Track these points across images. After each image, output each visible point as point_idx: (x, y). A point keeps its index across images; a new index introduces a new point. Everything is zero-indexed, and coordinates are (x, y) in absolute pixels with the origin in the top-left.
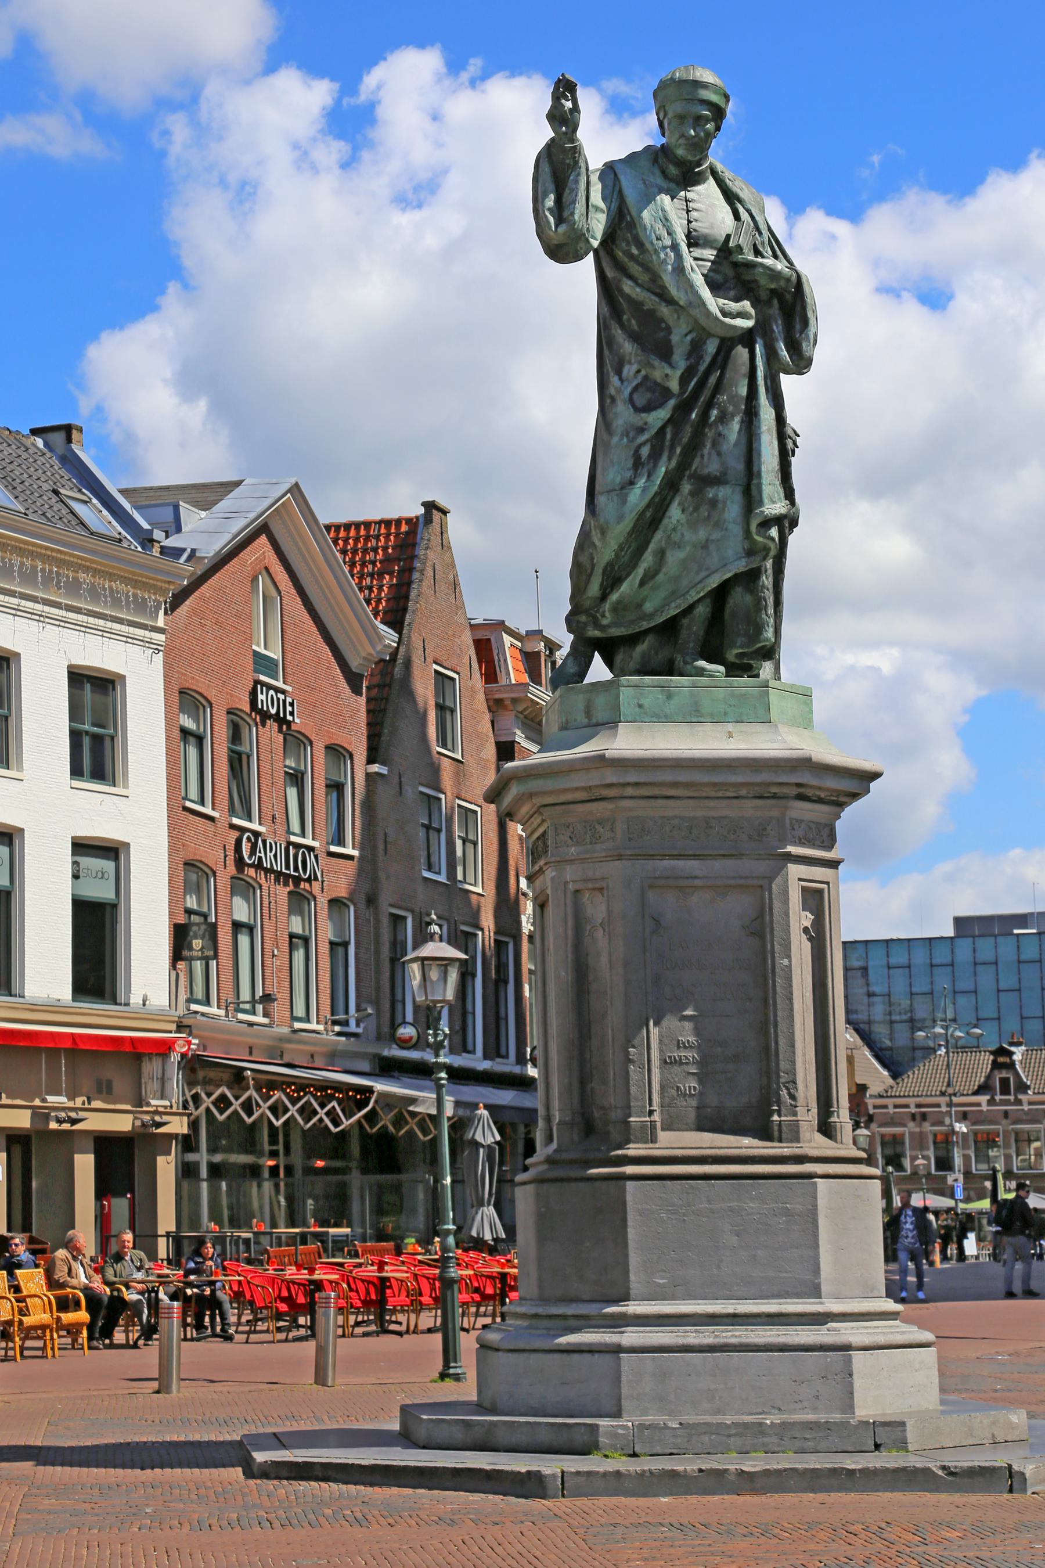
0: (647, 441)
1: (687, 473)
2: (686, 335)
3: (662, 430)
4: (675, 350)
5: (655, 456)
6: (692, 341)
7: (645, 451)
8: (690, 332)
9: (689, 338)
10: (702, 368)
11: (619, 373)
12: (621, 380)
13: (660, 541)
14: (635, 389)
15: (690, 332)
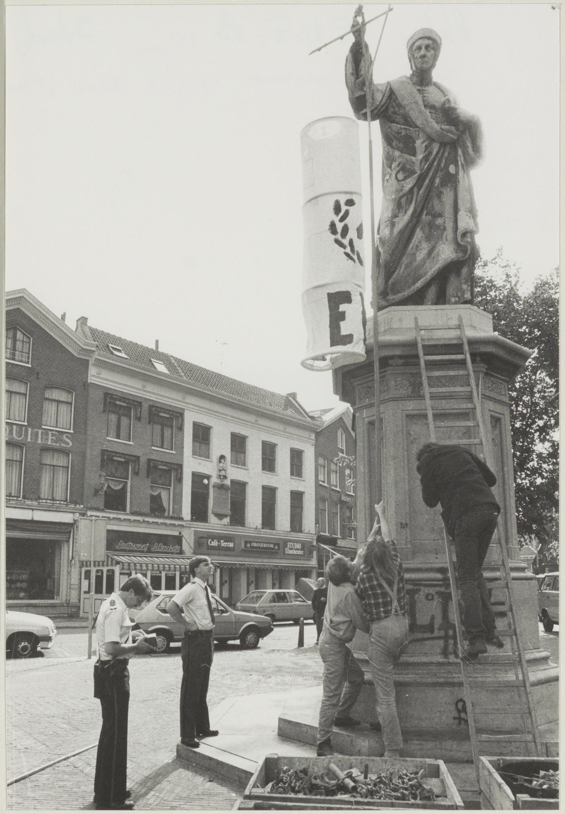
0: (404, 195)
1: (425, 212)
2: (423, 143)
3: (412, 189)
4: (417, 151)
5: (409, 202)
6: (426, 146)
7: (403, 200)
8: (424, 141)
9: (424, 145)
10: (431, 158)
11: (390, 167)
12: (391, 170)
13: (412, 248)
14: (398, 172)
15: (424, 141)
